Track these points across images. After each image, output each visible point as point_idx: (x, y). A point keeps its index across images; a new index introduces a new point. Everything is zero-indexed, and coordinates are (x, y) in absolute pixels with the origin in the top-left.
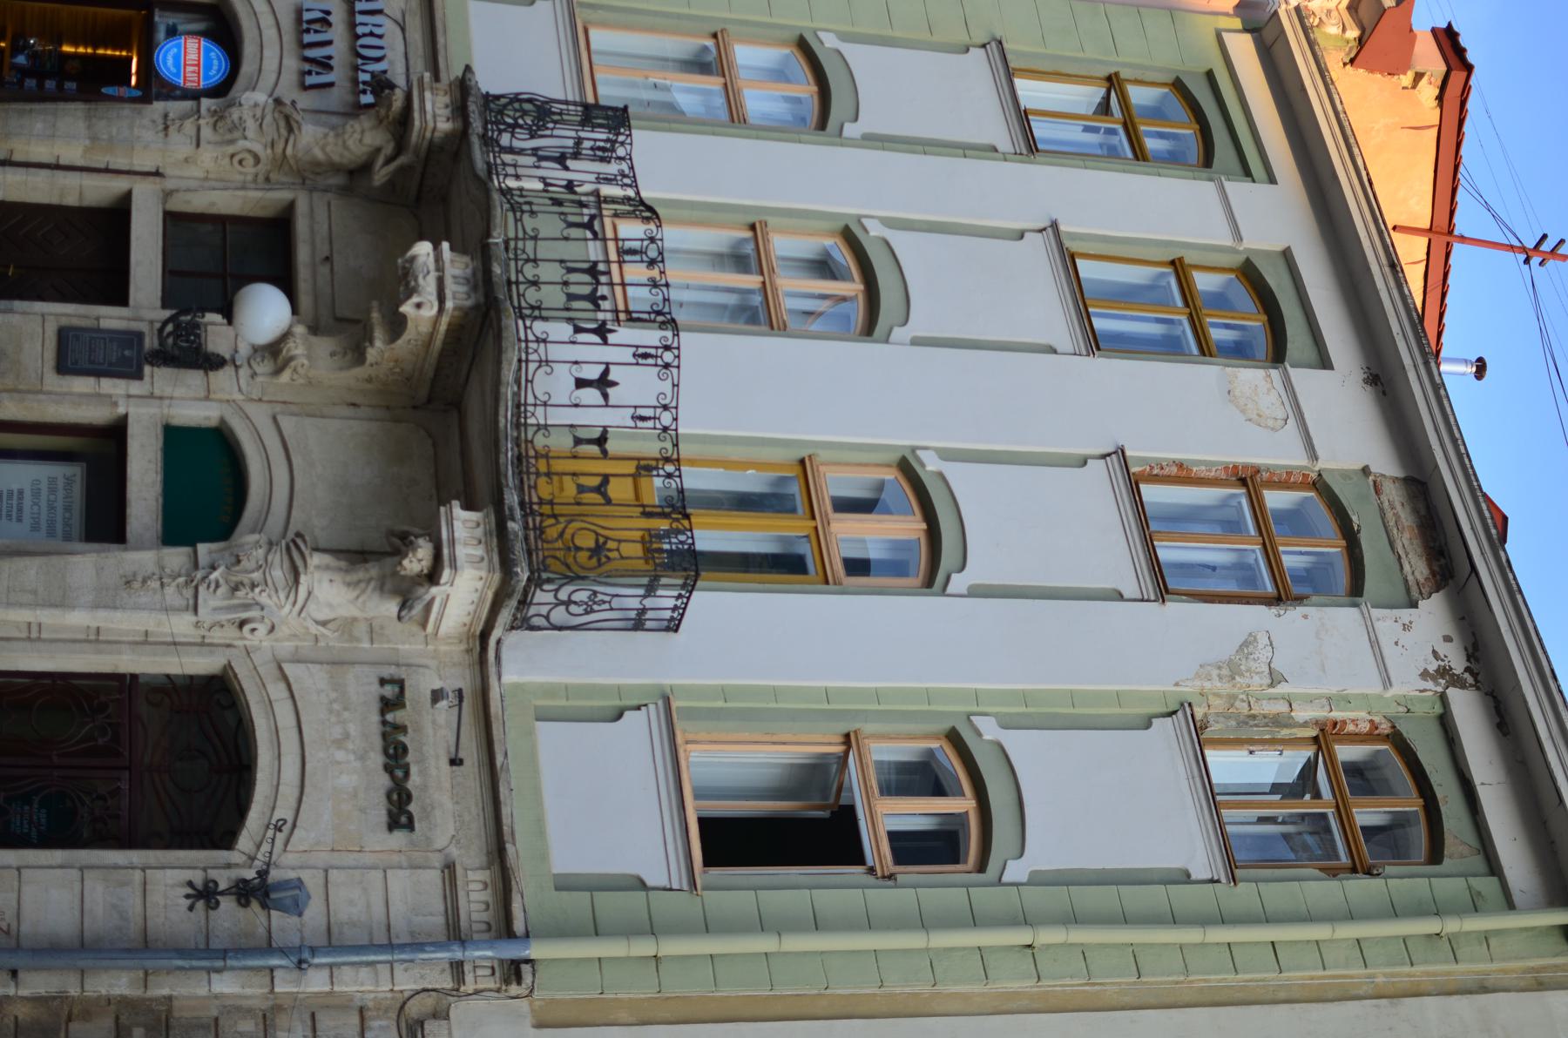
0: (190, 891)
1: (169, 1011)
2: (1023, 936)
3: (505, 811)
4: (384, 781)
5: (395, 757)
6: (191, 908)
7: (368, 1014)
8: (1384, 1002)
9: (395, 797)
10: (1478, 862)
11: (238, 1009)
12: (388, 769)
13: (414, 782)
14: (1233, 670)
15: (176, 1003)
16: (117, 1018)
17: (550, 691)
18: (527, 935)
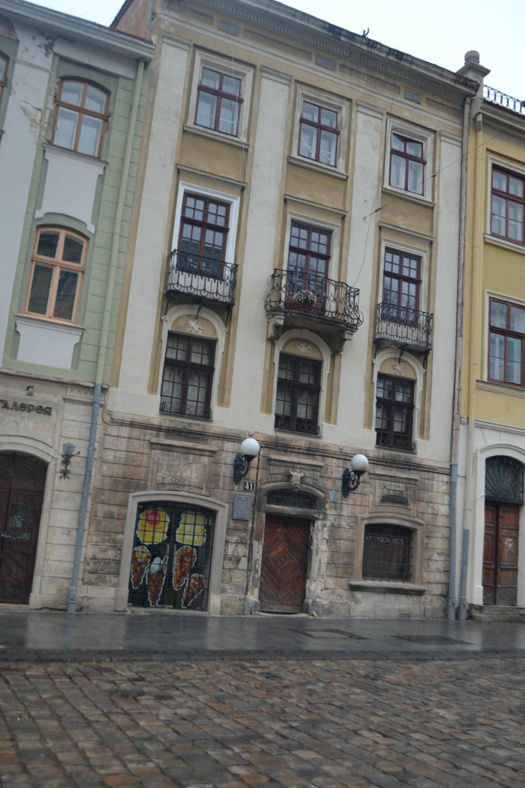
0: (63, 478)
1: (98, 488)
2: (117, 238)
3: (51, 379)
4: (34, 413)
5: (25, 408)
6: (68, 478)
7: (106, 433)
8: (151, 138)
9: (39, 411)
10: (113, 80)
11: (100, 469)
12: (29, 411)
14: (33, 121)
15: (96, 486)
16: (98, 503)
17: (5, 352)
18: (95, 383)
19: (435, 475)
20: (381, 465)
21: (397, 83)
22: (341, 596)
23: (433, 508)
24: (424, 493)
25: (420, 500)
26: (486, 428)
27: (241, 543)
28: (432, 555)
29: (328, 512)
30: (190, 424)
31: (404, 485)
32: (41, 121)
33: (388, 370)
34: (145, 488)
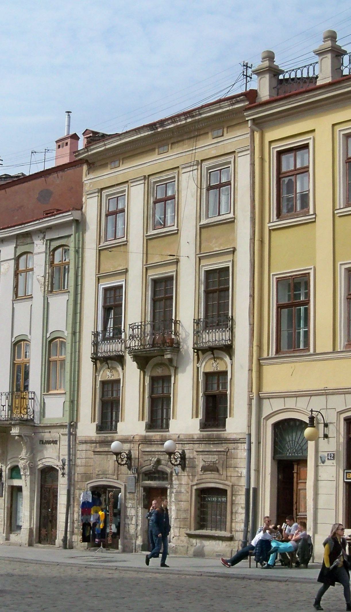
13: (51, 439)
19: (239, 444)
20: (203, 443)
21: (206, 130)
22: (183, 541)
23: (238, 472)
24: (231, 460)
25: (227, 467)
26: (272, 398)
27: (133, 507)
28: (238, 509)
29: (174, 482)
30: (107, 437)
31: (217, 456)
32: (45, 282)
33: (208, 370)
34: (92, 479)
